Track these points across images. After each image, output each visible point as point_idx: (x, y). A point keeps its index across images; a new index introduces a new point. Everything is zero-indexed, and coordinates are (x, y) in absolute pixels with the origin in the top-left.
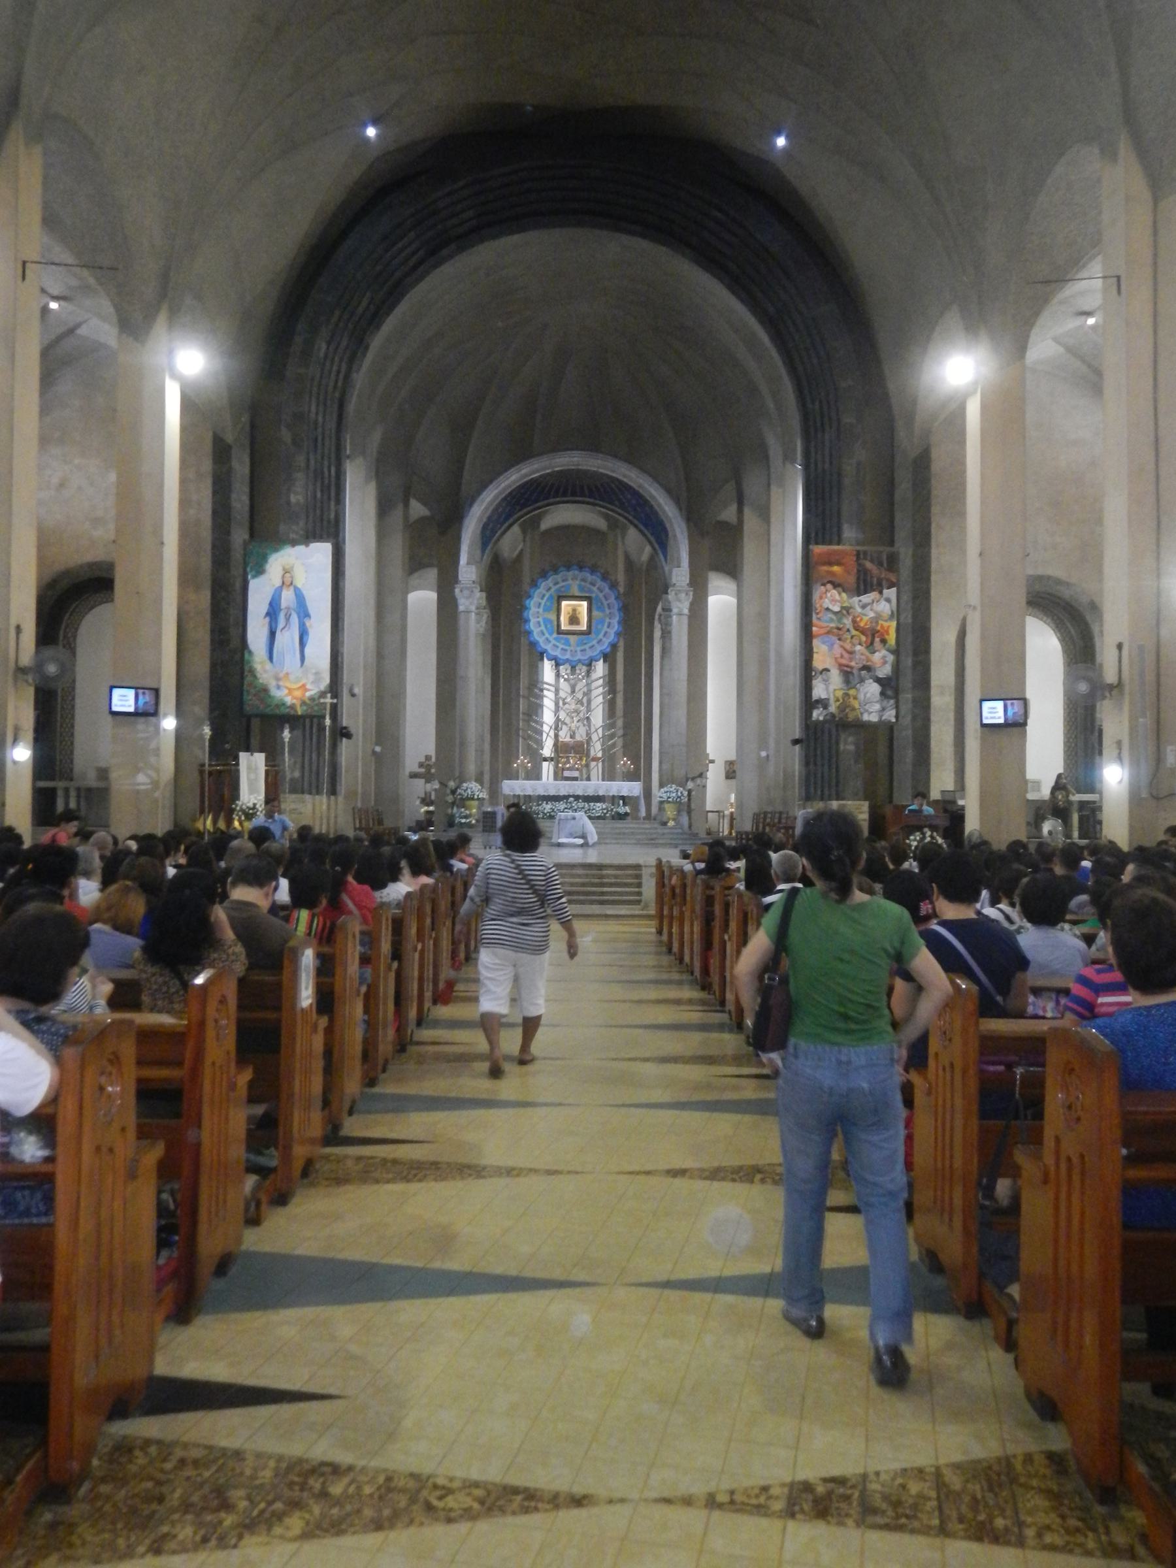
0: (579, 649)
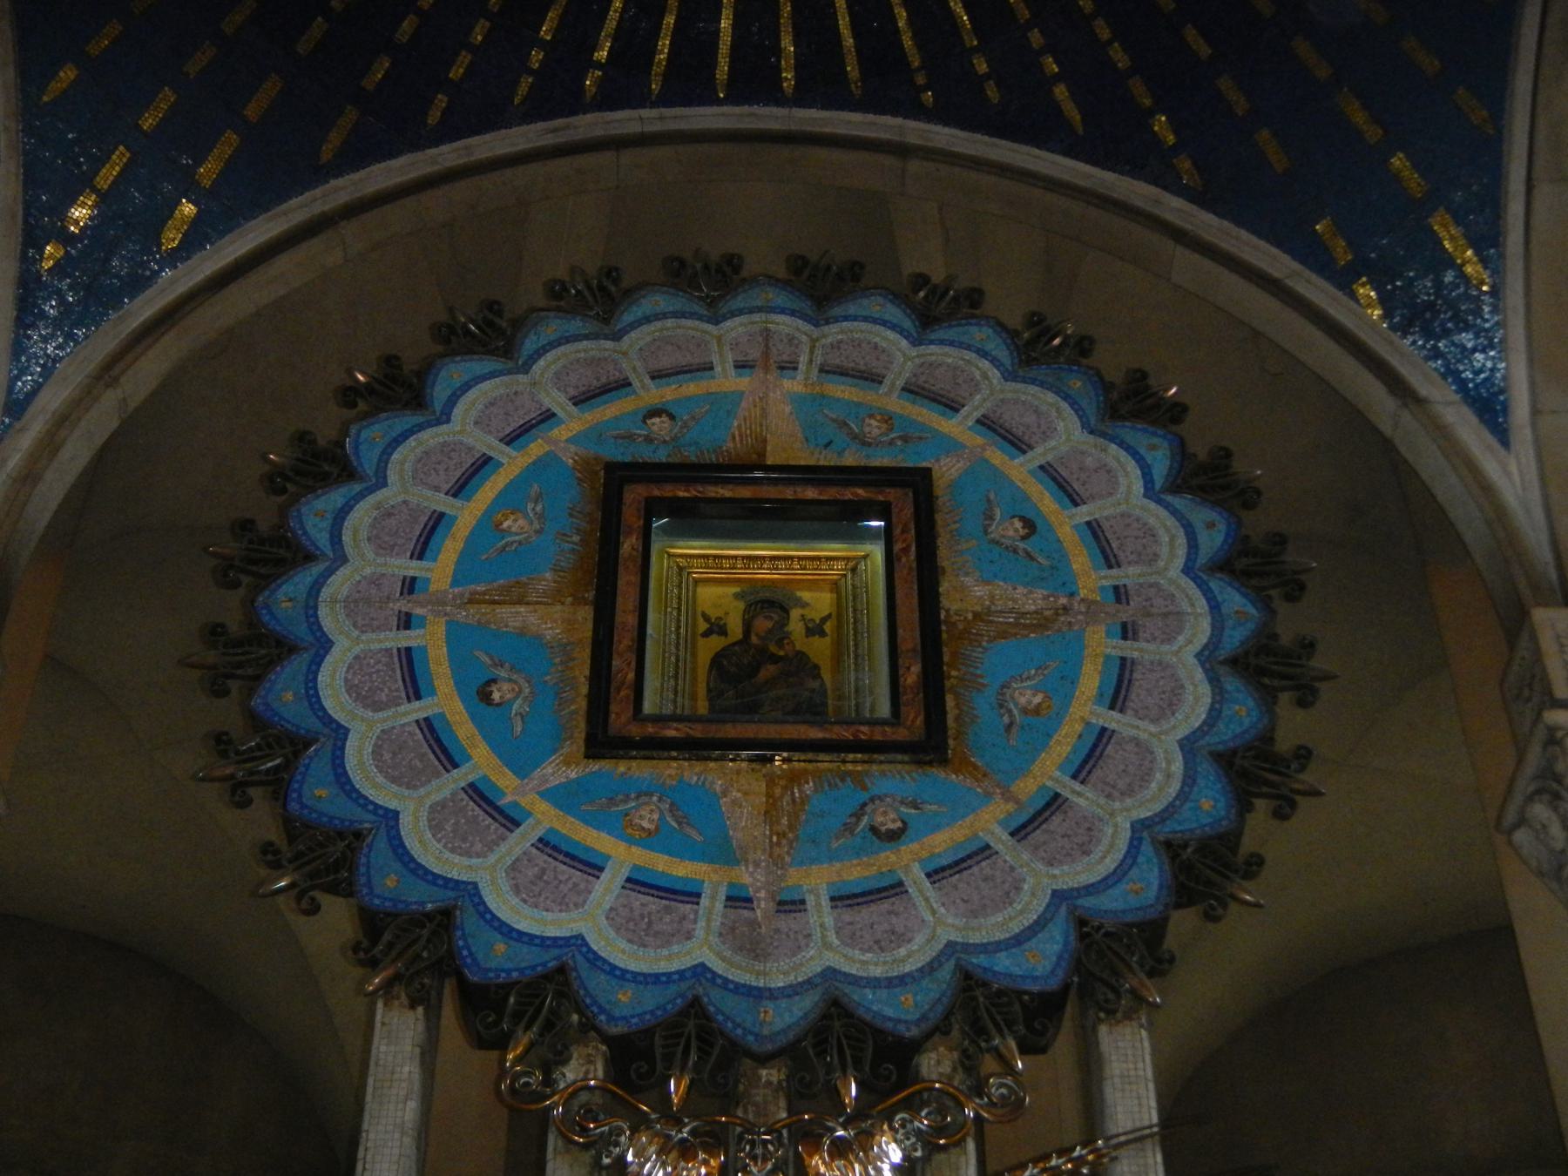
0: (816, 881)
